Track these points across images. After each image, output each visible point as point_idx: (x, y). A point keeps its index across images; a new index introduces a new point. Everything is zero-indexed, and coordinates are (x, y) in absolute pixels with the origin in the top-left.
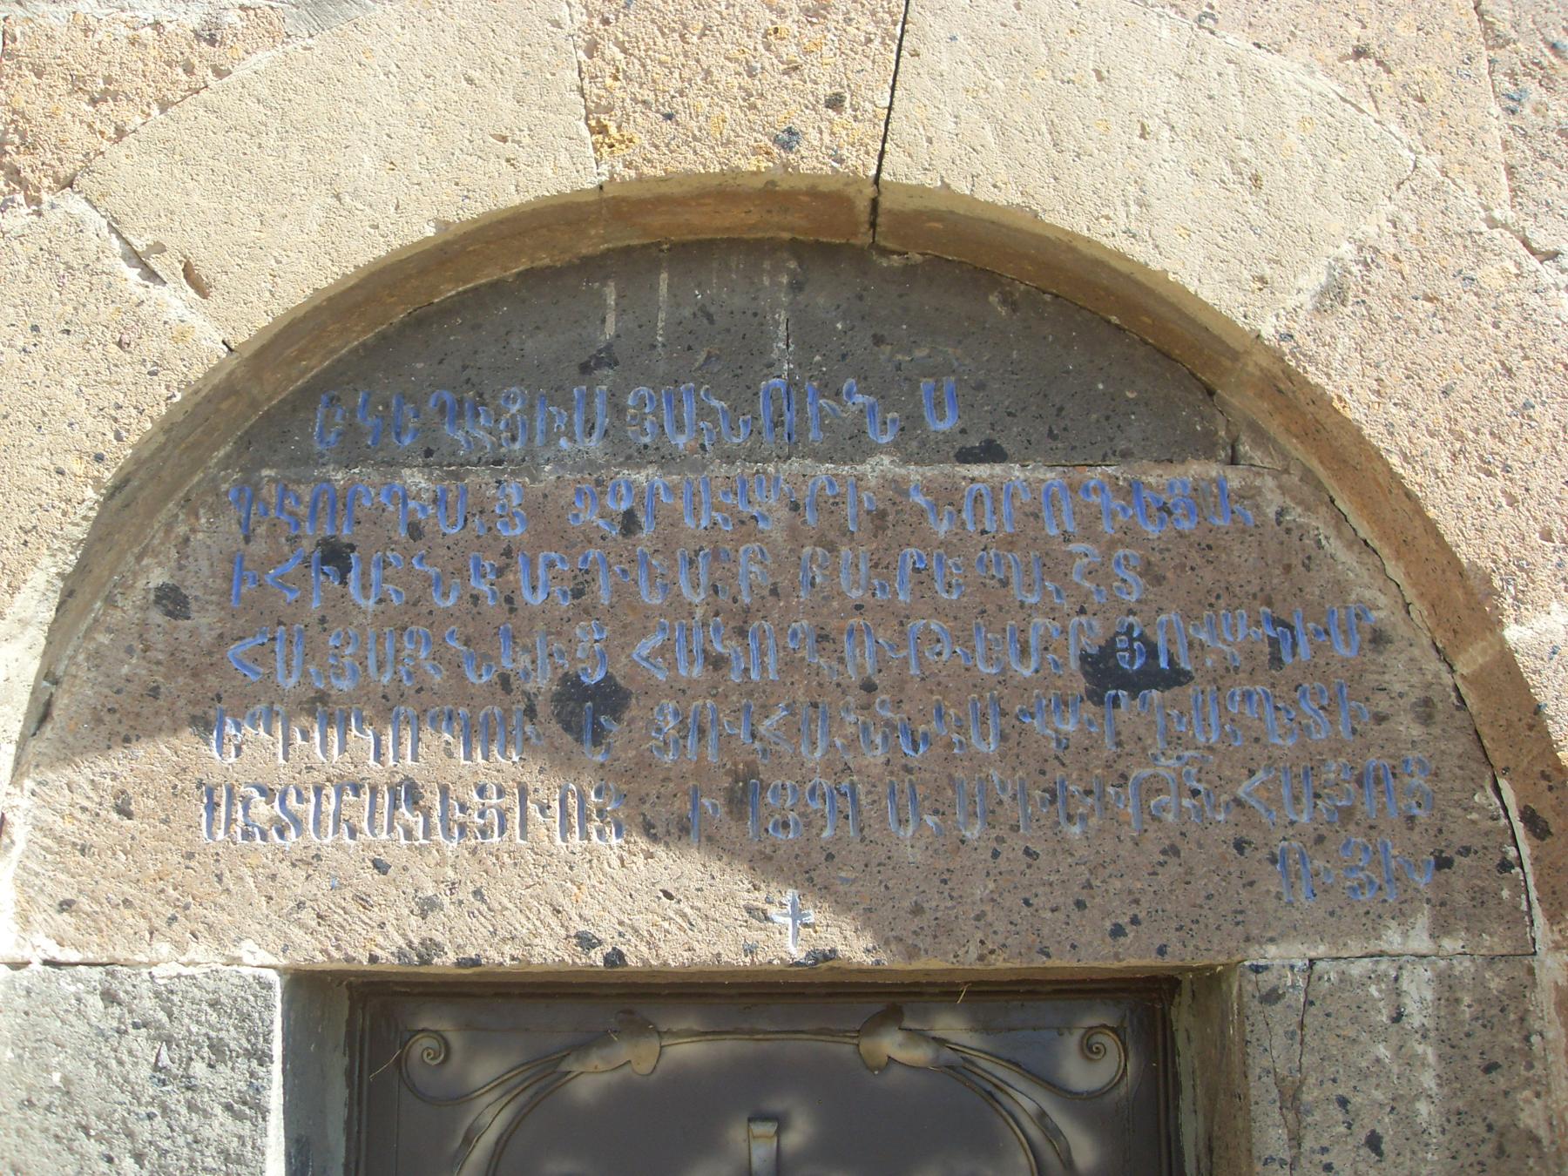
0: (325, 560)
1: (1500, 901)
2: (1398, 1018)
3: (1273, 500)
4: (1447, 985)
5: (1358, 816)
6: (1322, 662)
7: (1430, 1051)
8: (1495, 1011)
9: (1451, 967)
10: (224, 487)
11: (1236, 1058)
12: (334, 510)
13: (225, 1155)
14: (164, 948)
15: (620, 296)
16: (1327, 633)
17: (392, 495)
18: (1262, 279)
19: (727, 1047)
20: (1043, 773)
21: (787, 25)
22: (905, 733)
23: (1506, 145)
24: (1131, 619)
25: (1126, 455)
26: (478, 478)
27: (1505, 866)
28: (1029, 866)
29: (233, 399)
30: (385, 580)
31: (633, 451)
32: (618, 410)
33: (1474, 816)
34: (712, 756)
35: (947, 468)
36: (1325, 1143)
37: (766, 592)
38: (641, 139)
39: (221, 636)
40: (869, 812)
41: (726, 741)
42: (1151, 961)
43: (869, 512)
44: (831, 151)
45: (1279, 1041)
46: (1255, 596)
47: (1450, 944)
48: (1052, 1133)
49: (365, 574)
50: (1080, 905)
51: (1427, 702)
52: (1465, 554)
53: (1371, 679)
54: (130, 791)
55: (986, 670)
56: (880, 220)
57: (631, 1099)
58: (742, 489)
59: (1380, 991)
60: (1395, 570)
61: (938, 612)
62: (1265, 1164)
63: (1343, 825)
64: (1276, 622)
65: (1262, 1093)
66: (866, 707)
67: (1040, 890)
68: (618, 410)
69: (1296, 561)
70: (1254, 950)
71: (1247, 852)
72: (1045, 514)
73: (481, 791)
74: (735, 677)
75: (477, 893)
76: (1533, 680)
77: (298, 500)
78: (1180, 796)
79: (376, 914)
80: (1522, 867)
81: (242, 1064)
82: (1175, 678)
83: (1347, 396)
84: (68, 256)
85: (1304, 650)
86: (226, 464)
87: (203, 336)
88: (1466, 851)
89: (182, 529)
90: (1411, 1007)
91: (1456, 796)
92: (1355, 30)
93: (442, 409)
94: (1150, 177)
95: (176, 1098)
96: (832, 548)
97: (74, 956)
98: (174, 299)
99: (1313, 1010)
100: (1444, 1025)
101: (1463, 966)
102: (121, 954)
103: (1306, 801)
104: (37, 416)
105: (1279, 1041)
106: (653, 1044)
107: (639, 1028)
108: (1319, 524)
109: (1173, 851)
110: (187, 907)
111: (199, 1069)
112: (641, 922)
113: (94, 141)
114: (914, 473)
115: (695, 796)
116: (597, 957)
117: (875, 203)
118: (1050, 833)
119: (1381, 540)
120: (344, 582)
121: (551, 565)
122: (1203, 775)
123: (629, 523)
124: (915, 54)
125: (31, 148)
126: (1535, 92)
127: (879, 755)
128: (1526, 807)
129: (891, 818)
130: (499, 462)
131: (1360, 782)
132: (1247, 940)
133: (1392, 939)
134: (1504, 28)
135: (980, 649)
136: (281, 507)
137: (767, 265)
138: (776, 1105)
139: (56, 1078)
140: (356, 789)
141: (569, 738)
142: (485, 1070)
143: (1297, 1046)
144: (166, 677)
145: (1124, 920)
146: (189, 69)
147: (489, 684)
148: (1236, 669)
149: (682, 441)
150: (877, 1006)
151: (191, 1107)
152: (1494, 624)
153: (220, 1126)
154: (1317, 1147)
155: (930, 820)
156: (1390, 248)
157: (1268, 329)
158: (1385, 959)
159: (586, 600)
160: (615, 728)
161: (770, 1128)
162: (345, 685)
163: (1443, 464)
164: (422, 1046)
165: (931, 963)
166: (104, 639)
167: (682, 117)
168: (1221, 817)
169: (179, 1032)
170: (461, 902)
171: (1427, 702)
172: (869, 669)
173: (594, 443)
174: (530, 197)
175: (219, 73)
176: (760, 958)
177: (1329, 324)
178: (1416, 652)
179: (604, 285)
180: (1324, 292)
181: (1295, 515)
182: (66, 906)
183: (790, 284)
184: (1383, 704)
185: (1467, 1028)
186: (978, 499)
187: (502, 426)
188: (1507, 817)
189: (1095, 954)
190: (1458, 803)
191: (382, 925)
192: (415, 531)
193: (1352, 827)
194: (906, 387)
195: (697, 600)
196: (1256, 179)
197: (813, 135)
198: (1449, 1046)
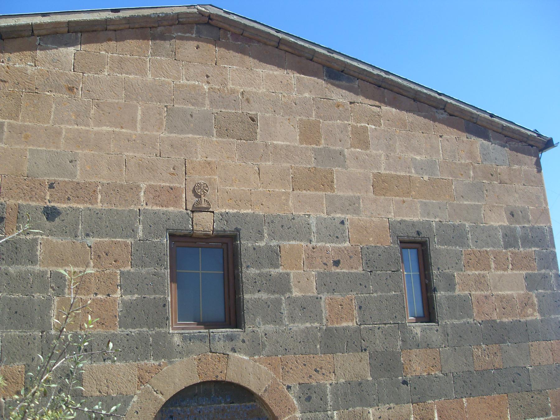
26: (185, 408)
44: (221, 377)
58: (210, 408)
87: (164, 399)
98: (160, 396)
108: (263, 408)
114: (226, 405)
192: (179, 414)
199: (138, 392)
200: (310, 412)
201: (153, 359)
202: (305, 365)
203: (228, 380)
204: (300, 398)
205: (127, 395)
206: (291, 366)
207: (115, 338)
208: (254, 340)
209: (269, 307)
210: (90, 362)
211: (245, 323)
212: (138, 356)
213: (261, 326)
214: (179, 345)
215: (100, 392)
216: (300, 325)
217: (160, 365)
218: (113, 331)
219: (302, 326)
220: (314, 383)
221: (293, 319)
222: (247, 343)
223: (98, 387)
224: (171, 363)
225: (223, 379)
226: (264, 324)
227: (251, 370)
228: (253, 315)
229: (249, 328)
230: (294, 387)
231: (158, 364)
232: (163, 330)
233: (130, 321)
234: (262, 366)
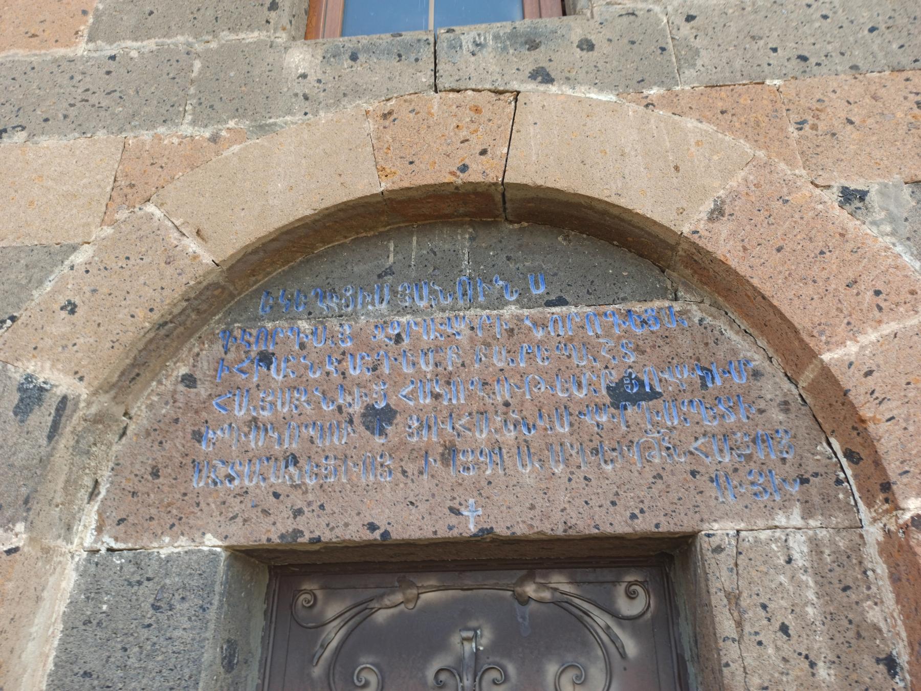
0: (260, 360)
1: (839, 500)
2: (789, 561)
4: (816, 546)
5: (755, 458)
6: (728, 386)
7: (810, 579)
8: (845, 558)
9: (816, 534)
10: (217, 331)
11: (703, 585)
12: (266, 339)
15: (396, 246)
16: (729, 372)
20: (591, 441)
22: (524, 425)
24: (630, 370)
26: (333, 323)
28: (587, 485)
29: (220, 290)
30: (287, 367)
31: (400, 309)
32: (394, 292)
33: (818, 457)
34: (435, 439)
35: (541, 309)
36: (757, 630)
37: (459, 365)
39: (210, 395)
40: (508, 462)
43: (506, 330)
44: (482, 172)
45: (725, 574)
46: (691, 357)
47: (812, 523)
50: (613, 503)
51: (786, 403)
53: (754, 394)
54: (160, 466)
56: (508, 205)
59: (778, 547)
60: (762, 342)
62: (724, 641)
63: (747, 463)
64: (703, 369)
65: (718, 601)
67: (593, 497)
70: (706, 526)
71: (698, 477)
72: (587, 327)
73: (327, 458)
74: (445, 403)
77: (250, 335)
78: (660, 450)
79: (271, 519)
80: (848, 482)
83: (728, 255)
85: (718, 382)
86: (218, 322)
87: (204, 257)
90: (796, 555)
91: (806, 447)
93: (317, 295)
94: (627, 172)
98: (192, 245)
99: (741, 557)
100: (816, 565)
101: (822, 534)
104: (124, 293)
105: (725, 574)
110: (180, 519)
114: (526, 312)
116: (377, 535)
117: (503, 195)
118: (596, 469)
119: (752, 327)
120: (269, 369)
121: (363, 358)
122: (671, 440)
123: (398, 339)
128: (846, 449)
129: (519, 464)
130: (341, 316)
131: (754, 441)
132: (702, 520)
135: (559, 387)
137: (459, 231)
139: (105, 607)
141: (368, 433)
142: (332, 610)
143: (735, 576)
144: (183, 414)
145: (637, 512)
147: (333, 410)
148: (684, 390)
149: (423, 304)
154: (752, 632)
156: (743, 189)
157: (686, 229)
158: (778, 530)
159: (378, 372)
160: (390, 428)
166: (155, 398)
168: (683, 460)
170: (313, 511)
171: (786, 403)
176: (455, 533)
178: (778, 380)
179: (389, 241)
180: (712, 212)
181: (709, 320)
183: (470, 238)
184: (762, 405)
185: (829, 567)
186: (555, 321)
187: (343, 301)
188: (836, 457)
190: (808, 451)
191: (274, 524)
192: (302, 346)
193: (752, 464)
194: (521, 276)
195: (428, 370)
196: (677, 168)
201: (194, 123)
214: (304, 76)
217: (214, 139)
224: (262, 129)
225: (494, 176)
231: (207, 135)
234: (690, 123)
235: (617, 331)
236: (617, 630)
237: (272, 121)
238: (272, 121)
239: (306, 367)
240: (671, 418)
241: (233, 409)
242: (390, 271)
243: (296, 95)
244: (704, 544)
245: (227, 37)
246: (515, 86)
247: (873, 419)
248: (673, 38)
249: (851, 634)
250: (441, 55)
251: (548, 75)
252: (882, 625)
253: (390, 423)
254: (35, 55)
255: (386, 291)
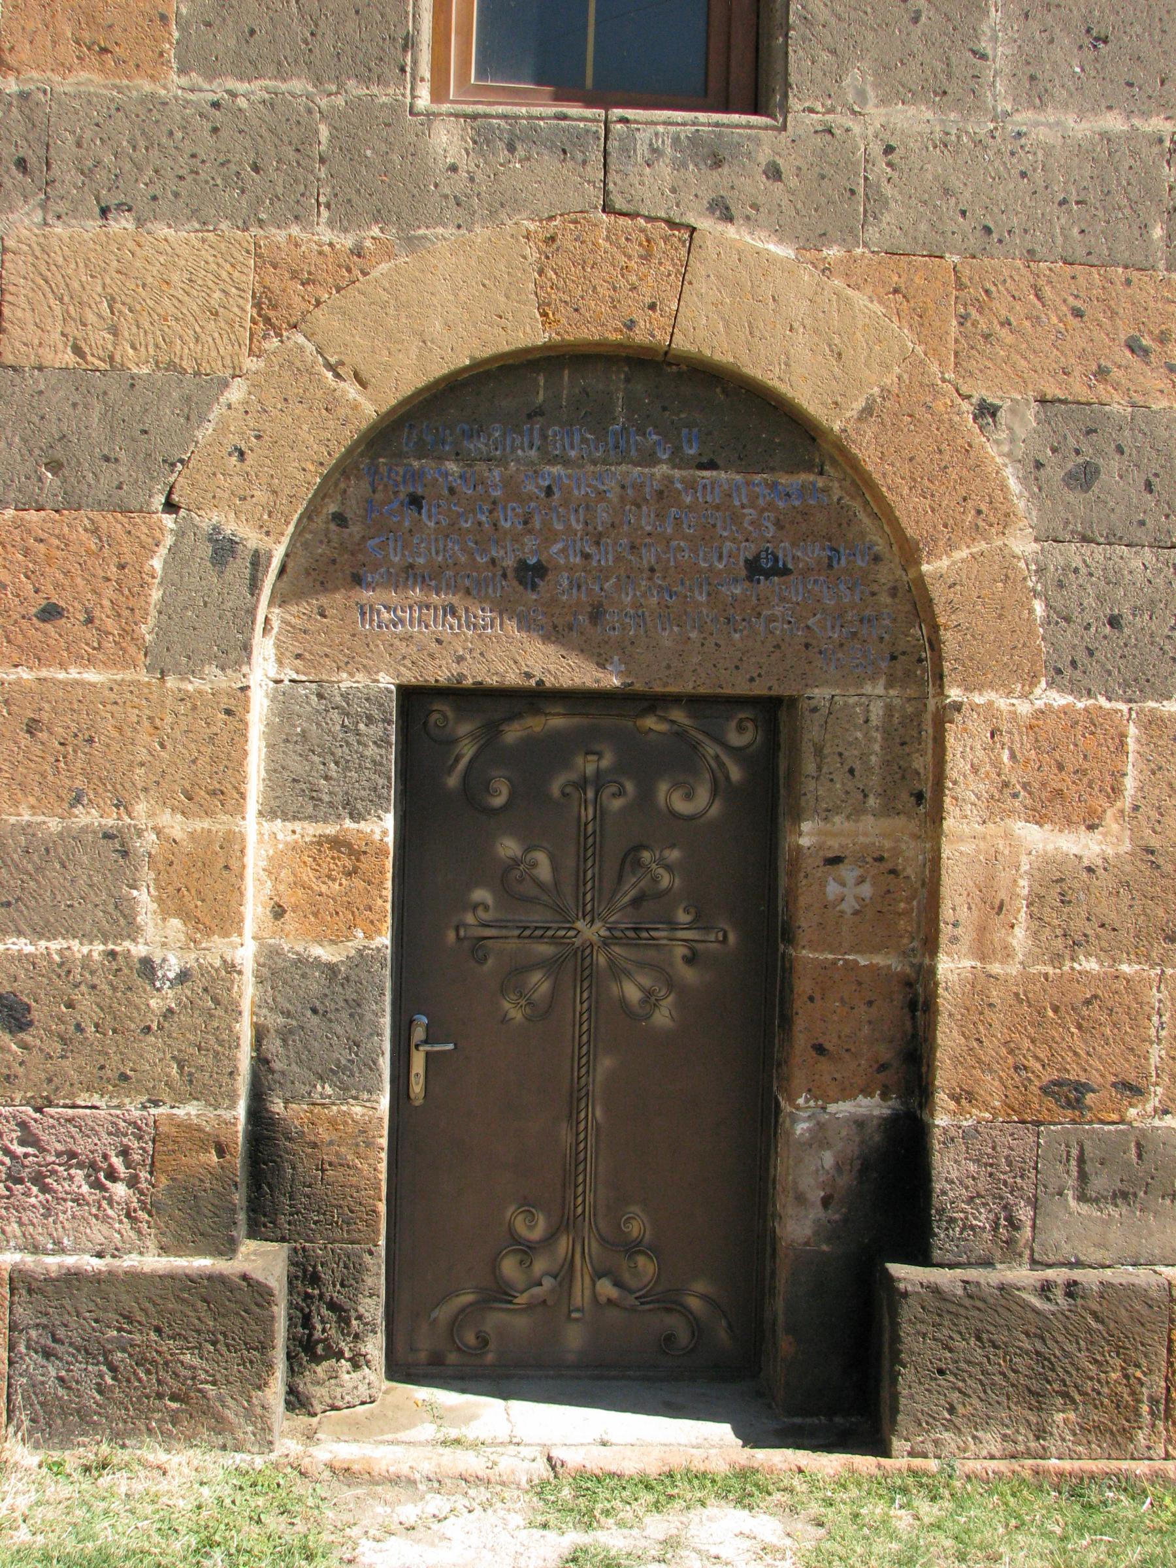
2: (867, 721)
3: (837, 493)
4: (889, 709)
13: (374, 762)
14: (345, 675)
17: (441, 474)
18: (836, 403)
19: (575, 721)
21: (632, 264)
23: (956, 341)
25: (773, 469)
26: (481, 467)
27: (920, 660)
32: (544, 437)
34: (583, 597)
38: (564, 321)
40: (650, 624)
41: (590, 591)
42: (765, 692)
44: (650, 332)
45: (816, 728)
47: (892, 692)
48: (721, 765)
49: (429, 510)
50: (737, 668)
52: (909, 532)
53: (871, 577)
55: (704, 565)
57: (530, 743)
60: (886, 528)
61: (685, 538)
64: (832, 549)
65: (807, 750)
66: (650, 579)
68: (544, 437)
69: (844, 522)
74: (594, 564)
75: (482, 654)
76: (930, 587)
81: (380, 725)
82: (786, 572)
84: (299, 364)
85: (843, 562)
86: (362, 455)
87: (367, 407)
88: (904, 653)
89: (342, 485)
90: (873, 717)
92: (896, 278)
95: (352, 739)
96: (639, 506)
97: (304, 678)
98: (351, 390)
101: (897, 702)
102: (325, 677)
103: (837, 628)
106: (543, 719)
107: (536, 711)
109: (778, 646)
111: (362, 726)
112: (552, 667)
113: (304, 306)
114: (677, 473)
115: (575, 614)
116: (533, 682)
121: (513, 509)
123: (549, 491)
124: (690, 283)
125: (275, 307)
126: (974, 313)
127: (655, 600)
131: (861, 621)
133: (868, 689)
134: (965, 280)
136: (389, 477)
138: (597, 747)
140: (428, 608)
142: (464, 729)
146: (349, 270)
149: (573, 453)
150: (646, 704)
151: (359, 742)
152: (920, 564)
153: (372, 751)
155: (676, 629)
157: (837, 427)
161: (595, 758)
162: (421, 561)
163: (906, 491)
164: (435, 717)
165: (673, 689)
166: (309, 536)
167: (583, 311)
169: (353, 712)
171: (895, 588)
172: (653, 561)
173: (533, 453)
174: (513, 347)
175: (365, 274)
177: (864, 426)
181: (846, 500)
182: (298, 656)
184: (875, 588)
186: (705, 487)
189: (742, 688)
192: (452, 491)
196: (840, 354)
197: (642, 323)
198: (887, 733)
199: (251, 364)
200: (1085, 539)
201: (331, 223)
202: (1078, 313)
203: (683, 344)
204: (1039, 465)
205: (197, 374)
206: (1004, 313)
207: (156, 115)
208: (829, 171)
209: (916, 20)
210: (38, 217)
211: (787, 85)
212: (260, 201)
213: (870, 109)
214: (454, 168)
215: (78, 351)
216: (1070, 120)
217: (358, 252)
218: (147, 87)
219: (1082, 128)
220: (1118, 406)
221: (1034, 89)
222: (793, 182)
223: (71, 329)
224: (411, 243)
226: (883, 102)
227: (799, 309)
228: (834, 52)
229: (804, 112)
230: (1013, 411)
232: (383, 95)
233: (232, 43)
234: (859, 299)
235: (761, 502)
236: (725, 758)
237: (421, 232)
238: (421, 232)
239: (459, 515)
240: (797, 593)
241: (387, 555)
242: (539, 412)
243: (446, 197)
244: (804, 705)
245: (355, 88)
246: (691, 219)
247: (945, 625)
248: (866, 179)
249: (897, 776)
250: (612, 159)
251: (727, 208)
252: (922, 771)
253: (542, 578)
254: (115, 86)
255: (536, 434)
